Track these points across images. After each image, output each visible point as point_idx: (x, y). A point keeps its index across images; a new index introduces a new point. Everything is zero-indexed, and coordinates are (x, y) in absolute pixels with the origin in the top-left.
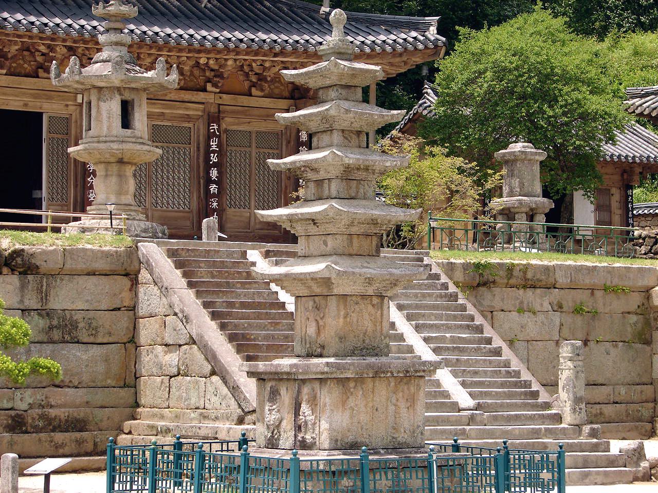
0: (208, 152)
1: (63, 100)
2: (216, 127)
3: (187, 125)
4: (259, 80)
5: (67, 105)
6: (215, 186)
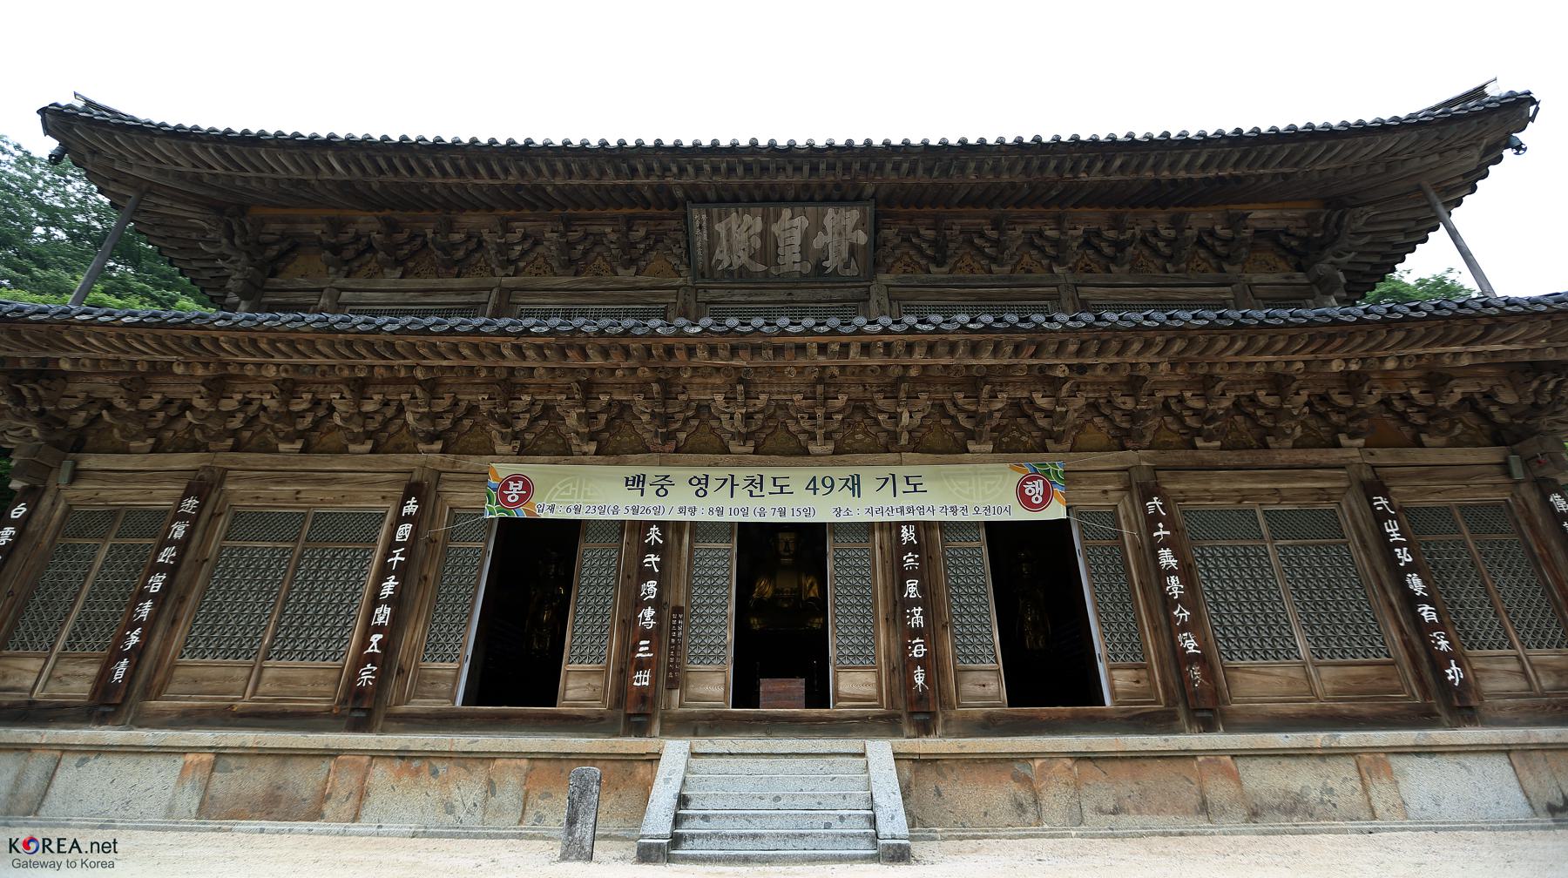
0: (1388, 547)
1: (1096, 483)
2: (1385, 502)
3: (1325, 506)
4: (1429, 419)
5: (1105, 492)
6: (1427, 607)
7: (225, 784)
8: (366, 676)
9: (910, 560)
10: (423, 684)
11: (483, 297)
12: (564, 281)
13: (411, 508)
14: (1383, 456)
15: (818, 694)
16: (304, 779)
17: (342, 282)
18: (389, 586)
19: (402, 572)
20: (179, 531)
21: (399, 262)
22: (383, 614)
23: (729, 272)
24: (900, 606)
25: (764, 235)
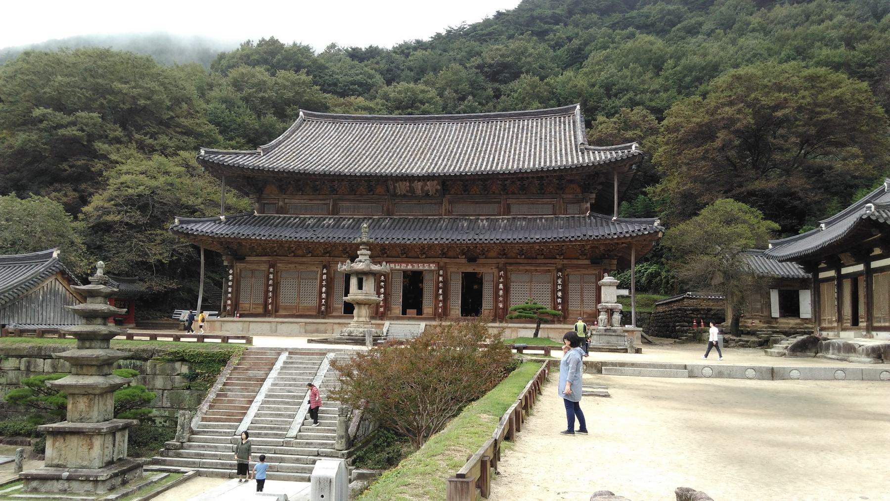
7: (309, 327)
8: (323, 308)
9: (441, 285)
10: (335, 309)
11: (328, 202)
12: (352, 197)
13: (325, 271)
14: (565, 262)
15: (420, 312)
16: (322, 327)
17: (284, 196)
18: (324, 289)
19: (326, 286)
20: (271, 276)
21: (301, 190)
22: (324, 296)
23: (400, 195)
24: (437, 295)
25: (410, 186)
